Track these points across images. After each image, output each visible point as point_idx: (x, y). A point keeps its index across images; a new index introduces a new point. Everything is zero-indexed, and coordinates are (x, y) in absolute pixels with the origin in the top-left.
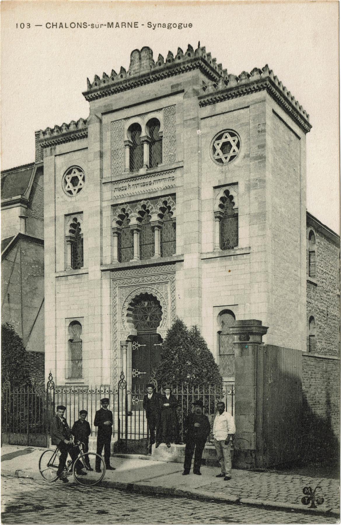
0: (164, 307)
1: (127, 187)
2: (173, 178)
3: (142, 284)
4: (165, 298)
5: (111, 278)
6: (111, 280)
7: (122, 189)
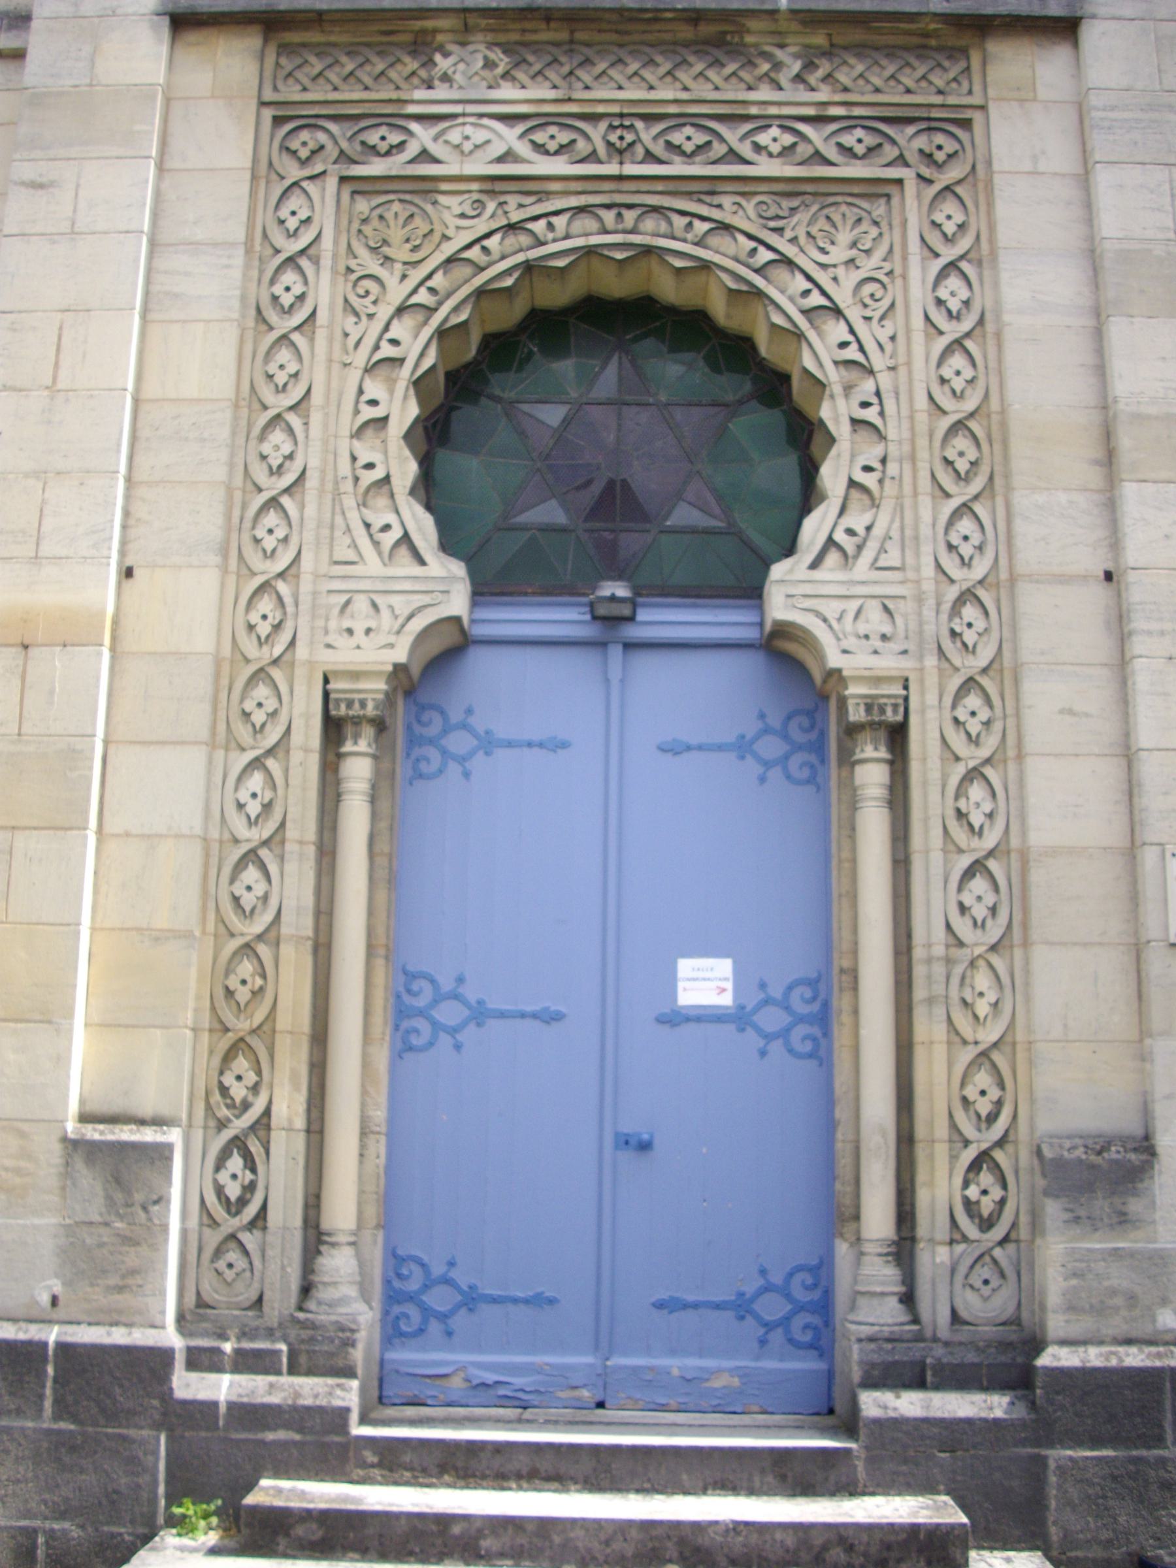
0: (848, 389)
3: (612, 169)
4: (854, 314)
5: (269, 95)
6: (268, 114)
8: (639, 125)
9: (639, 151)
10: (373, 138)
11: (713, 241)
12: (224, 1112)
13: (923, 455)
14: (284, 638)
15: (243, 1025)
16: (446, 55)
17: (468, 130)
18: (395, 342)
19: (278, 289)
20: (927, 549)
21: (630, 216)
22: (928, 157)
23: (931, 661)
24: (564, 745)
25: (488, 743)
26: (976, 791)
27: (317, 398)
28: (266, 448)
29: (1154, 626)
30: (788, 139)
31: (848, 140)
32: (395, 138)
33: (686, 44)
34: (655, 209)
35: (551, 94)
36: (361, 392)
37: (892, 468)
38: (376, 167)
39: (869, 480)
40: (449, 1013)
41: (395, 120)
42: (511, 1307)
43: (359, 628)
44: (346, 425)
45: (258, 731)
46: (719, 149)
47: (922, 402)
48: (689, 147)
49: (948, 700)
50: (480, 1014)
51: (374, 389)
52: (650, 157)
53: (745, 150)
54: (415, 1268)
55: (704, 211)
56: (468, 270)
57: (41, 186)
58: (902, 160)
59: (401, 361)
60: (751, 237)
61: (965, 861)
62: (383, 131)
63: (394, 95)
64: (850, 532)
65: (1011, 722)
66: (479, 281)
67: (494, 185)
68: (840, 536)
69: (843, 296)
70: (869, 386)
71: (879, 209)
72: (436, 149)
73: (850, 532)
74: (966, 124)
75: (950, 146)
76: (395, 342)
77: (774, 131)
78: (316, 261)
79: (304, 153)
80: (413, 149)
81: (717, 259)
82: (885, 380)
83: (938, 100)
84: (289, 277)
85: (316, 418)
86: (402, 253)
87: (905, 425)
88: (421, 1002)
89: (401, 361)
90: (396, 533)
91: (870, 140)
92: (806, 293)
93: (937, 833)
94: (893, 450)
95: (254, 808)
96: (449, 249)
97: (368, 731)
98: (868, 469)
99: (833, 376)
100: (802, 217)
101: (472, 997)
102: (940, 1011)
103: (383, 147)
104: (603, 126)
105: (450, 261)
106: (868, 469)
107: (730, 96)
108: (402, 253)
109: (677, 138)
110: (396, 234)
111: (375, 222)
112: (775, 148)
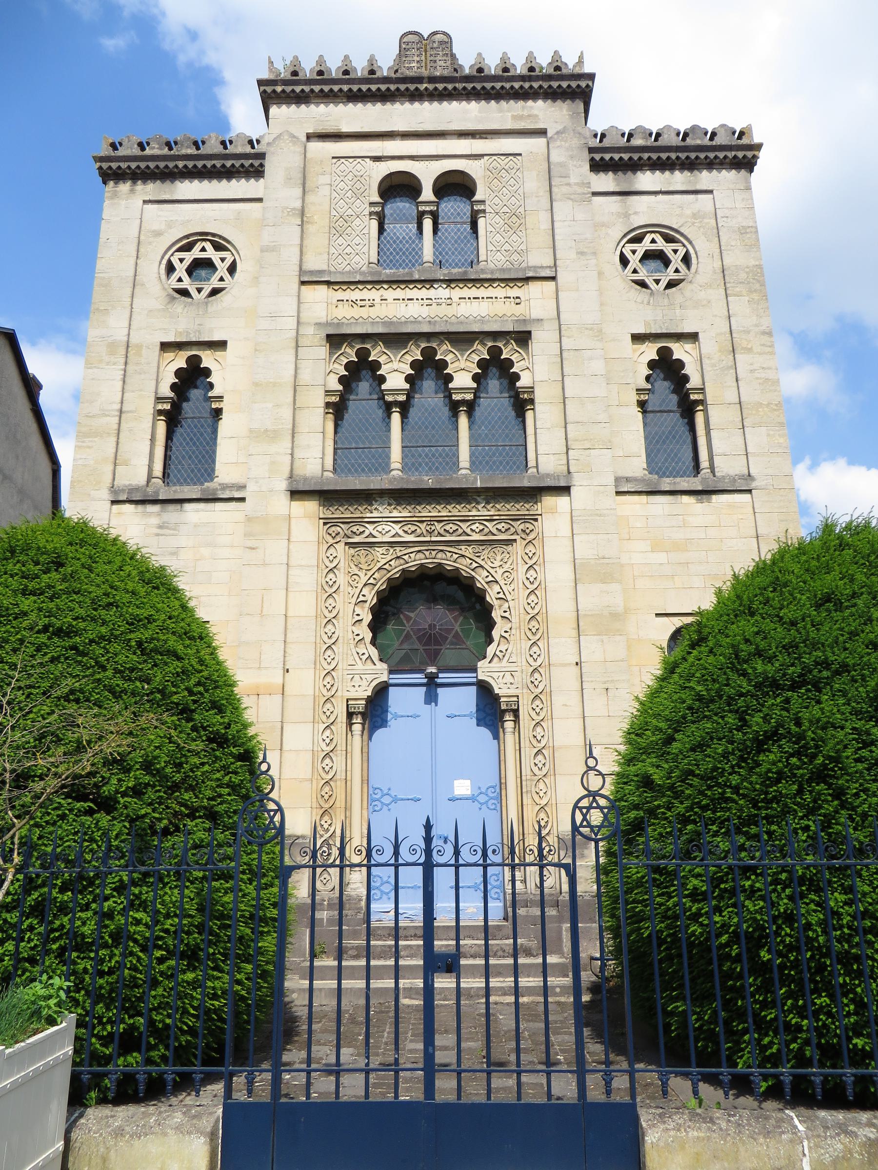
0: (500, 606)
1: (378, 300)
2: (518, 301)
3: (428, 539)
4: (502, 583)
6: (322, 521)
7: (363, 303)
8: (436, 523)
9: (436, 532)
10: (354, 529)
11: (459, 560)
12: (322, 833)
13: (522, 627)
14: (334, 689)
15: (327, 806)
16: (376, 501)
17: (384, 526)
18: (364, 596)
19: (328, 580)
20: (523, 657)
21: (434, 553)
22: (523, 531)
23: (525, 691)
24: (418, 716)
25: (396, 716)
26: (539, 729)
27: (341, 614)
28: (326, 630)
29: (590, 679)
30: (481, 527)
31: (500, 526)
32: (362, 529)
33: (450, 496)
34: (442, 551)
35: (409, 515)
36: (354, 611)
37: (513, 631)
38: (356, 539)
39: (506, 635)
40: (386, 800)
41: (360, 522)
42: (408, 890)
43: (357, 686)
44: (351, 621)
45: (328, 717)
46: (460, 531)
47: (522, 611)
48: (451, 531)
49: (530, 702)
50: (395, 800)
51: (358, 610)
52: (440, 535)
53: (468, 531)
54: (379, 879)
55: (456, 551)
56: (385, 572)
57: (254, 549)
58: (516, 533)
59: (366, 601)
60: (470, 559)
61: (536, 750)
62: (358, 527)
63: (361, 515)
64: (501, 651)
65: (549, 708)
66: (388, 575)
67: (391, 544)
68: (498, 653)
69: (498, 578)
70: (506, 605)
71: (509, 548)
72: (375, 533)
73: (501, 651)
74: (536, 520)
75: (531, 527)
76: (364, 596)
77: (477, 525)
78: (339, 570)
79: (334, 535)
80: (367, 533)
81: (460, 566)
82: (511, 603)
83: (527, 513)
84: (331, 575)
85: (341, 621)
86: (365, 567)
87: (517, 617)
88: (377, 797)
89: (366, 601)
90: (367, 656)
91: (507, 526)
92: (487, 577)
93: (527, 742)
94: (514, 626)
95: (328, 741)
96: (379, 565)
97: (359, 716)
98: (506, 632)
99: (496, 603)
100: (486, 552)
101: (393, 794)
102: (529, 795)
103: (358, 532)
104: (425, 524)
105: (379, 569)
106: (506, 632)
107: (463, 514)
108: (365, 567)
109: (447, 528)
110: (363, 560)
111: (356, 557)
112: (477, 530)
